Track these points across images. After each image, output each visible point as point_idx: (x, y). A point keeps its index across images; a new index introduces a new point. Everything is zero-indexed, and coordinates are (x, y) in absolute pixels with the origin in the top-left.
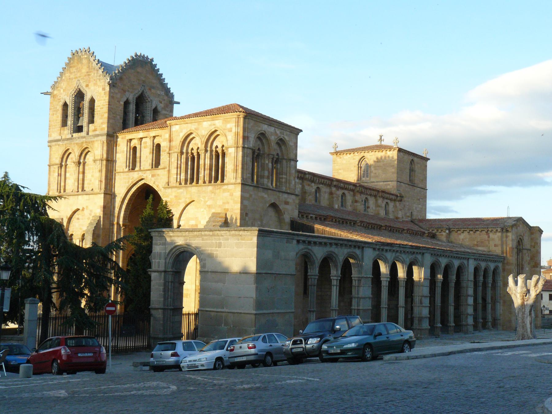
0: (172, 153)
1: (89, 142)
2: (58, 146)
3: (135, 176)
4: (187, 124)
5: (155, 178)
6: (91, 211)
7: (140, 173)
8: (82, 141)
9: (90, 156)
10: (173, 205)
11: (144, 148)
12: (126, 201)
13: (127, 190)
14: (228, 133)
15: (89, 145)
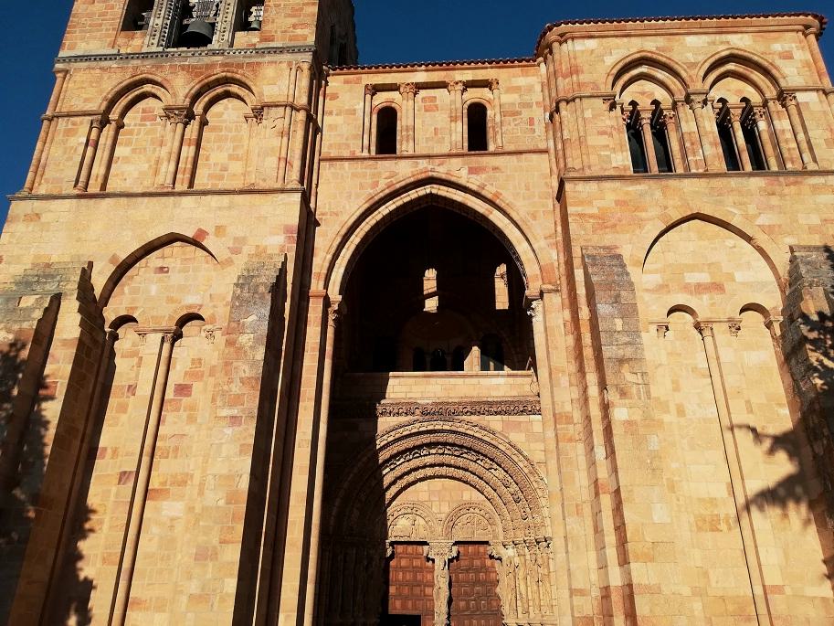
0: (581, 98)
1: (240, 66)
2: (98, 71)
3: (403, 171)
4: (625, 39)
5: (484, 176)
6: (240, 242)
7: (423, 164)
8: (209, 62)
9: (226, 108)
10: (614, 226)
11: (426, 111)
12: (355, 239)
13: (367, 206)
14: (778, 62)
15: (240, 71)
